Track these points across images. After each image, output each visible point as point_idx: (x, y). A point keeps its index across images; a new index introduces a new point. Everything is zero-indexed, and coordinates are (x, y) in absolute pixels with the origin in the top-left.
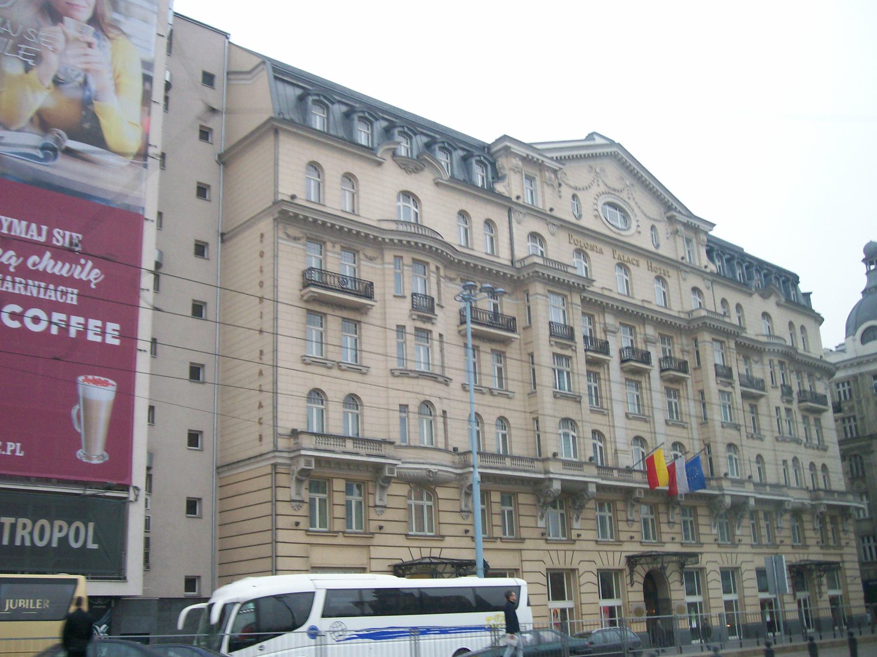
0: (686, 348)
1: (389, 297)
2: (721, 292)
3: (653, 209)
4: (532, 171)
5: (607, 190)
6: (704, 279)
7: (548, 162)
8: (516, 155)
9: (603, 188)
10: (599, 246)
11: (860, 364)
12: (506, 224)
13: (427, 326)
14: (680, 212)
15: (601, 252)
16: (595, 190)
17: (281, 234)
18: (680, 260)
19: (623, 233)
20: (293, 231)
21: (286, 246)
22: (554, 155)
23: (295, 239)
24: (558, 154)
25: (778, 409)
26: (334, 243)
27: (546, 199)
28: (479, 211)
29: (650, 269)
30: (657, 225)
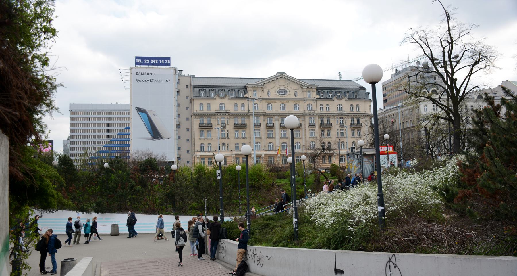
0: (303, 120)
1: (217, 125)
2: (319, 103)
3: (296, 87)
4: (255, 89)
7: (259, 86)
9: (278, 86)
10: (275, 101)
15: (276, 102)
16: (276, 87)
18: (304, 98)
20: (197, 117)
22: (261, 84)
25: (338, 130)
26: (205, 117)
27: (259, 94)
30: (297, 91)
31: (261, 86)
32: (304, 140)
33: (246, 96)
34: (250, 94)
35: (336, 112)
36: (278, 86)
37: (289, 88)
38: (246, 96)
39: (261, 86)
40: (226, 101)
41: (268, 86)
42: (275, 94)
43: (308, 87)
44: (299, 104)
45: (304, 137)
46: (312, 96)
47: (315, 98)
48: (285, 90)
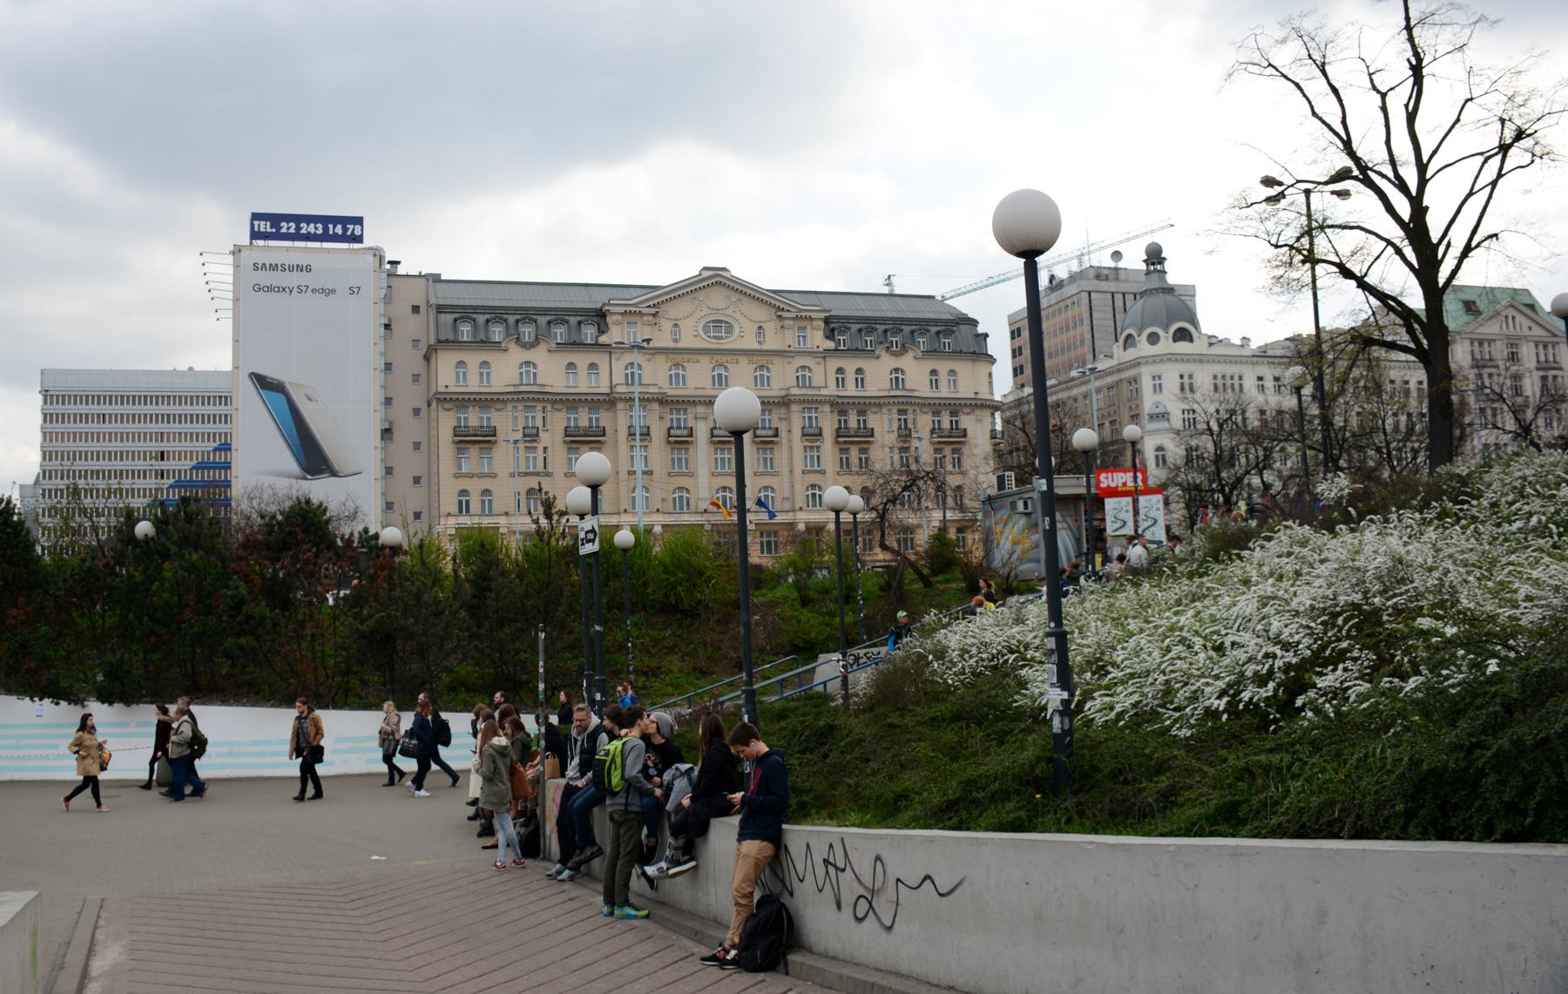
2: (834, 364)
3: (761, 314)
5: (710, 311)
6: (815, 357)
7: (643, 311)
8: (615, 313)
9: (706, 311)
11: (1118, 371)
12: (608, 363)
13: (534, 445)
14: (788, 311)
16: (698, 314)
17: (440, 409)
18: (787, 349)
19: (721, 341)
20: (447, 406)
21: (442, 414)
22: (651, 303)
23: (449, 410)
24: (655, 302)
28: (582, 360)
29: (751, 362)
31: (653, 311)
32: (786, 479)
33: (603, 339)
34: (614, 335)
35: (886, 394)
36: (706, 311)
37: (738, 315)
38: (603, 339)
39: (653, 311)
40: (539, 355)
41: (675, 310)
42: (696, 336)
43: (799, 314)
44: (770, 366)
45: (785, 471)
46: (812, 342)
47: (821, 349)
48: (726, 322)
